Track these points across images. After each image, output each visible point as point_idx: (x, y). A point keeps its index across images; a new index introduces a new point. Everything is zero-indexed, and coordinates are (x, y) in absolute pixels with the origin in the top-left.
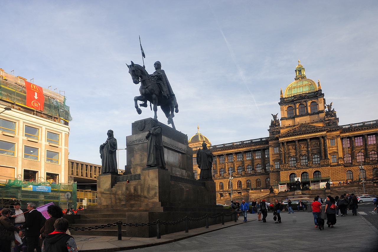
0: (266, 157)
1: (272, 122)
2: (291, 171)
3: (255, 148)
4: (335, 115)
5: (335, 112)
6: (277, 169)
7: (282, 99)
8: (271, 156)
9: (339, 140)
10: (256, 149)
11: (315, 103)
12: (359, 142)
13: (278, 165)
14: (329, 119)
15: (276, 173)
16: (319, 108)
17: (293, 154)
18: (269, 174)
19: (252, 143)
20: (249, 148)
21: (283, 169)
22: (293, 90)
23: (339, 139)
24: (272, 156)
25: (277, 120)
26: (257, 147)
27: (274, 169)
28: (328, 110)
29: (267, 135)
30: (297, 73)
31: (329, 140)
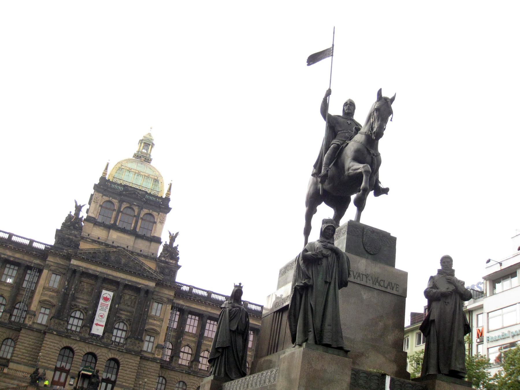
0: (25, 285)
1: (69, 217)
2: (67, 340)
4: (177, 259)
5: (178, 251)
6: (41, 324)
7: (103, 179)
8: (39, 289)
9: (169, 309)
10: (12, 259)
11: (152, 218)
13: (46, 317)
14: (167, 260)
15: (36, 333)
16: (155, 230)
17: (82, 303)
18: (19, 330)
21: (55, 331)
22: (127, 173)
23: (169, 307)
24: (42, 289)
25: (80, 216)
26: (18, 255)
27: (34, 323)
28: (168, 243)
30: (140, 146)
31: (154, 301)
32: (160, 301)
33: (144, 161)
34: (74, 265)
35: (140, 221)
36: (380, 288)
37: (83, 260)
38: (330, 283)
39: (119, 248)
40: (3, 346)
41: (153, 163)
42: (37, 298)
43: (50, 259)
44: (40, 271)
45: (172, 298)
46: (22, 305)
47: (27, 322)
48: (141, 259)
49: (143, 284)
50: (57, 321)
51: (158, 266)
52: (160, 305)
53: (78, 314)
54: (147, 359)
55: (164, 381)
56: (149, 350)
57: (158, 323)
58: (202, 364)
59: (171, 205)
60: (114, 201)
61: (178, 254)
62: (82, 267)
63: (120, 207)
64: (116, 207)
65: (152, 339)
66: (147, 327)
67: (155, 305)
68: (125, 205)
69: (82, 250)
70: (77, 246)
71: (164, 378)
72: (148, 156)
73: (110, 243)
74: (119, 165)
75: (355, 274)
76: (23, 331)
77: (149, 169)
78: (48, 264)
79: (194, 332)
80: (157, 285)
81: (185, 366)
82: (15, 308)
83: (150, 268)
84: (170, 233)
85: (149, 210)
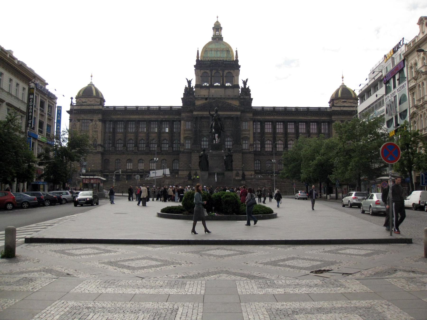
0: (175, 130)
1: (186, 89)
3: (163, 118)
4: (250, 95)
5: (250, 90)
6: (188, 149)
7: (198, 61)
8: (182, 132)
12: (268, 128)
13: (189, 145)
16: (234, 81)
18: (178, 154)
19: (160, 110)
20: (156, 117)
22: (210, 52)
23: (252, 123)
25: (192, 86)
26: (166, 117)
27: (184, 149)
28: (243, 87)
29: (179, 103)
32: (246, 121)
33: (219, 40)
34: (195, 115)
35: (225, 78)
37: (199, 111)
39: (216, 99)
40: (174, 164)
41: (225, 40)
42: (182, 137)
43: (183, 115)
44: (180, 121)
45: (252, 117)
46: (176, 141)
47: (181, 150)
48: (230, 101)
49: (234, 115)
50: (195, 146)
51: (240, 103)
52: (246, 123)
53: (205, 139)
54: (246, 153)
55: (259, 162)
56: (247, 148)
57: (248, 133)
58: (279, 148)
59: (240, 63)
60: (207, 71)
61: (250, 92)
62: (200, 114)
63: (211, 74)
64: (210, 75)
65: (247, 142)
66: (242, 136)
67: (244, 123)
68: (214, 72)
69: (197, 106)
70: (194, 104)
71: (259, 160)
72: (220, 36)
73: (211, 96)
74: (205, 49)
76: (180, 155)
77: (222, 45)
78: (182, 118)
79: (271, 131)
80: (241, 113)
81: (270, 151)
82: (173, 144)
83: (235, 105)
84: (243, 80)
85: (228, 70)
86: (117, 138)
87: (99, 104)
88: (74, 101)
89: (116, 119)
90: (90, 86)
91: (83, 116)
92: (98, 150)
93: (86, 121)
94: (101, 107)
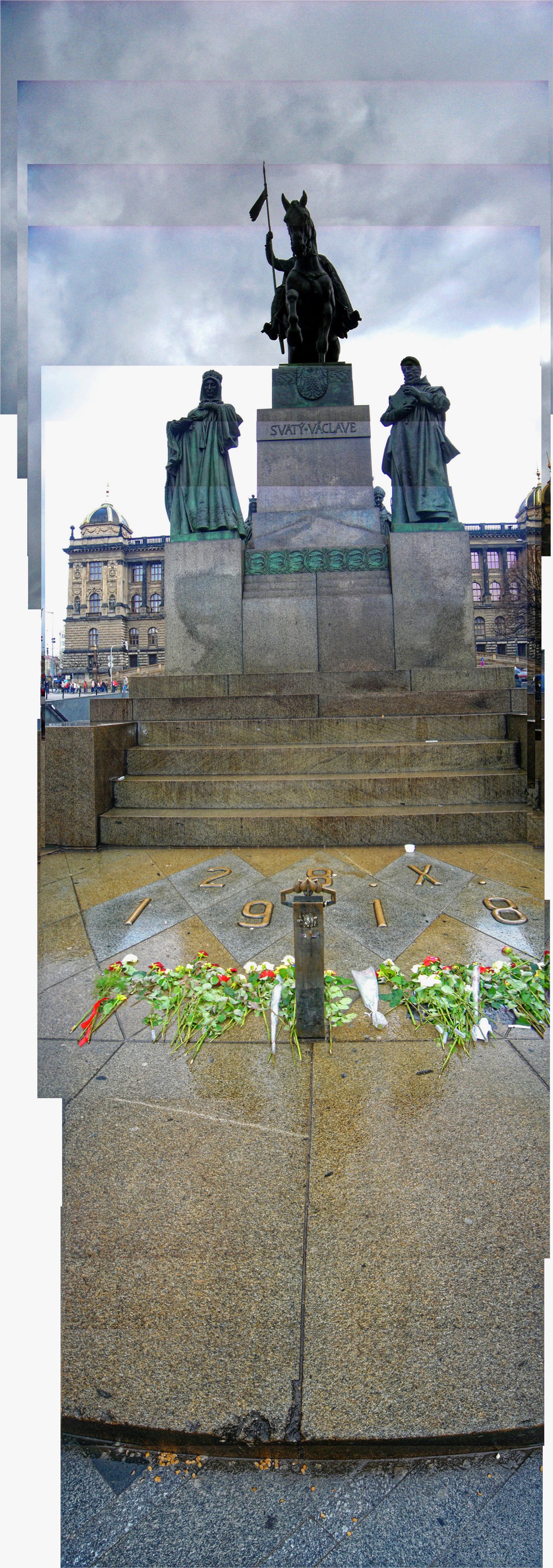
36: (325, 436)
38: (205, 448)
75: (282, 429)
86: (150, 592)
87: (117, 534)
88: (78, 534)
89: (147, 559)
90: (104, 506)
91: (90, 556)
92: (117, 614)
93: (96, 565)
94: (120, 540)
